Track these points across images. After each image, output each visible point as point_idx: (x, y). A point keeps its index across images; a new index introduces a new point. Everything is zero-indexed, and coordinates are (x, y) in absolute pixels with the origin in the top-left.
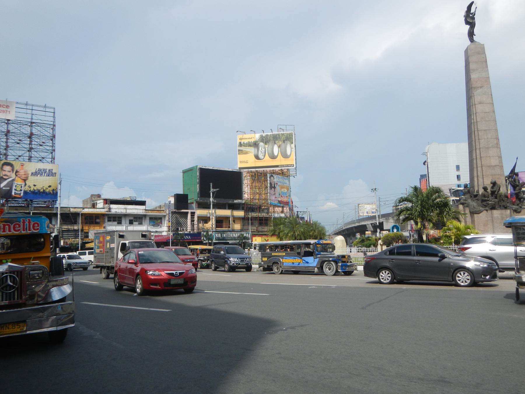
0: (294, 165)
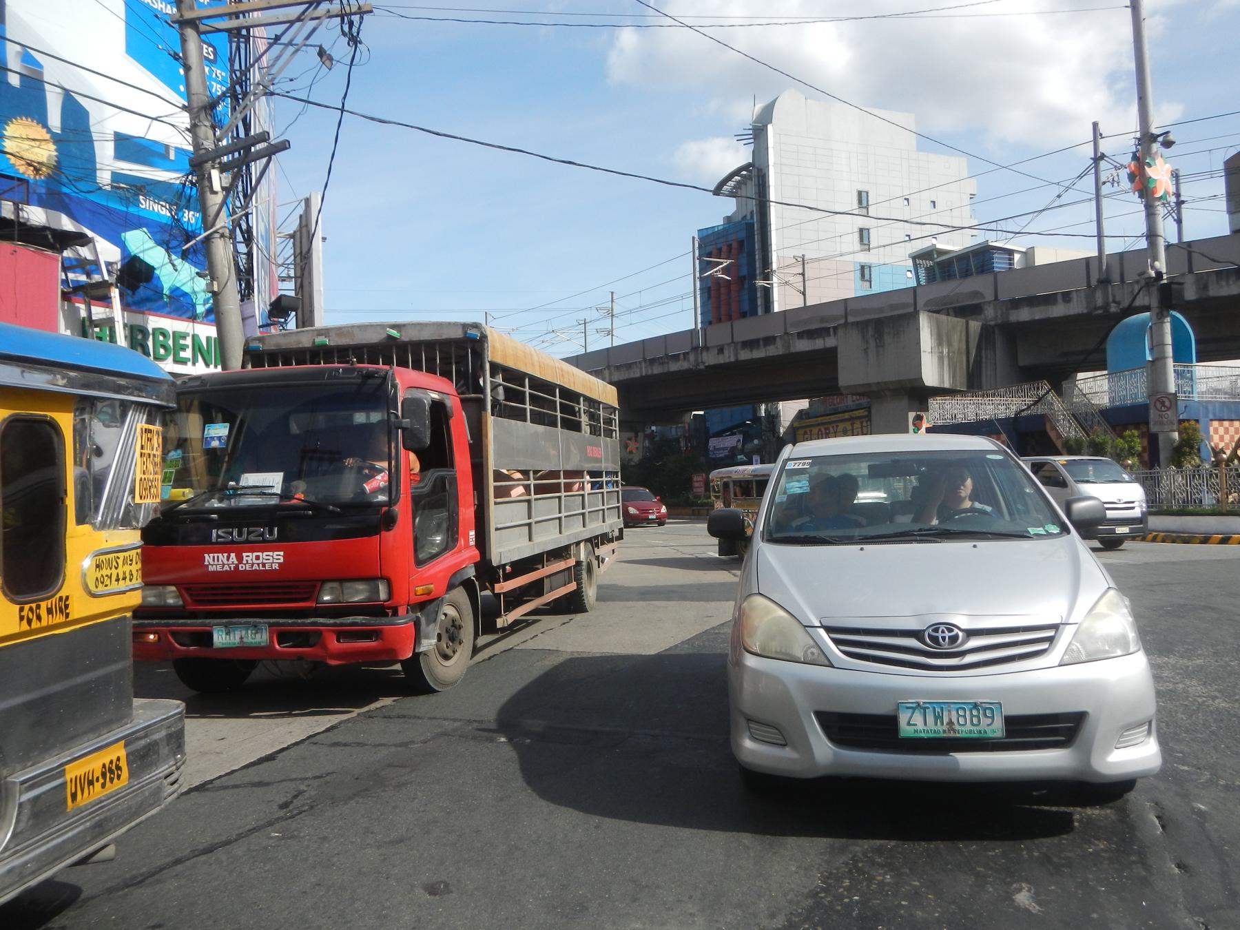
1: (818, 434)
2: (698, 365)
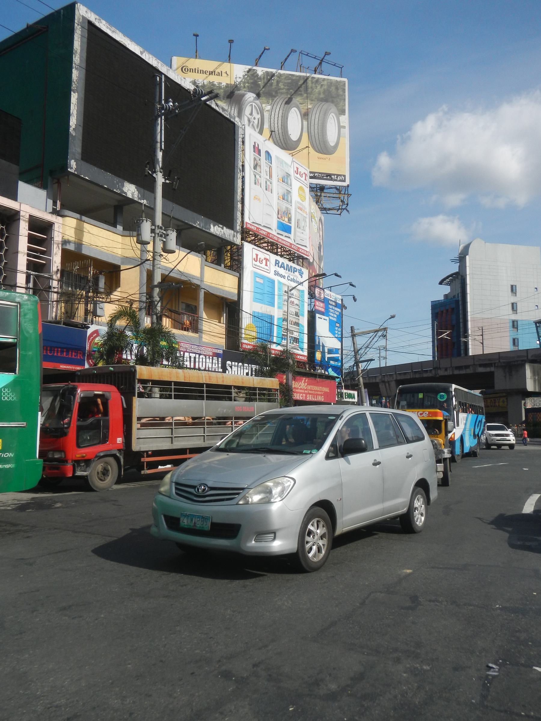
0: (344, 176)
1: (490, 403)
2: (436, 375)
